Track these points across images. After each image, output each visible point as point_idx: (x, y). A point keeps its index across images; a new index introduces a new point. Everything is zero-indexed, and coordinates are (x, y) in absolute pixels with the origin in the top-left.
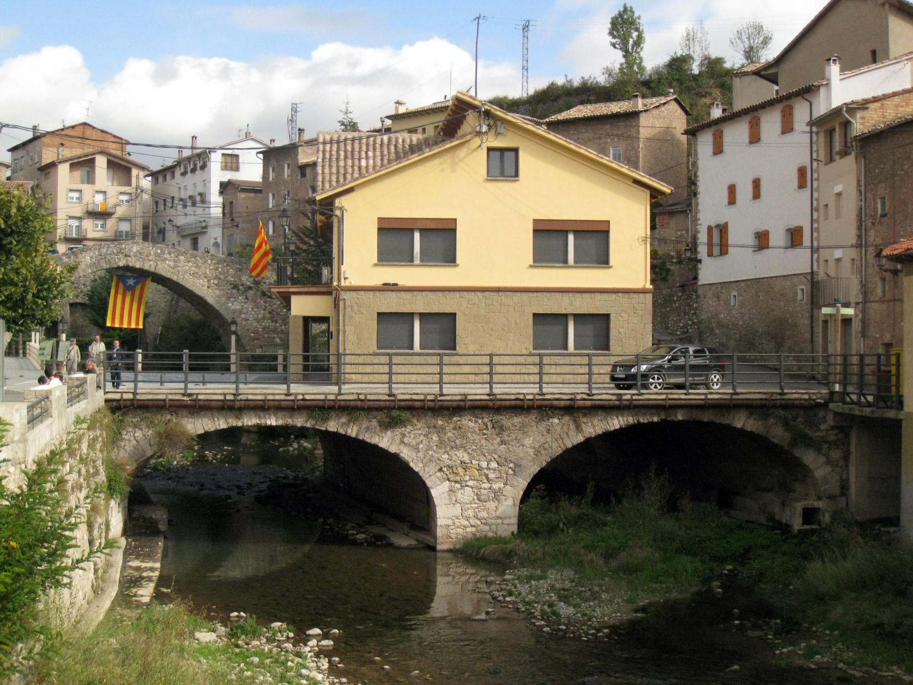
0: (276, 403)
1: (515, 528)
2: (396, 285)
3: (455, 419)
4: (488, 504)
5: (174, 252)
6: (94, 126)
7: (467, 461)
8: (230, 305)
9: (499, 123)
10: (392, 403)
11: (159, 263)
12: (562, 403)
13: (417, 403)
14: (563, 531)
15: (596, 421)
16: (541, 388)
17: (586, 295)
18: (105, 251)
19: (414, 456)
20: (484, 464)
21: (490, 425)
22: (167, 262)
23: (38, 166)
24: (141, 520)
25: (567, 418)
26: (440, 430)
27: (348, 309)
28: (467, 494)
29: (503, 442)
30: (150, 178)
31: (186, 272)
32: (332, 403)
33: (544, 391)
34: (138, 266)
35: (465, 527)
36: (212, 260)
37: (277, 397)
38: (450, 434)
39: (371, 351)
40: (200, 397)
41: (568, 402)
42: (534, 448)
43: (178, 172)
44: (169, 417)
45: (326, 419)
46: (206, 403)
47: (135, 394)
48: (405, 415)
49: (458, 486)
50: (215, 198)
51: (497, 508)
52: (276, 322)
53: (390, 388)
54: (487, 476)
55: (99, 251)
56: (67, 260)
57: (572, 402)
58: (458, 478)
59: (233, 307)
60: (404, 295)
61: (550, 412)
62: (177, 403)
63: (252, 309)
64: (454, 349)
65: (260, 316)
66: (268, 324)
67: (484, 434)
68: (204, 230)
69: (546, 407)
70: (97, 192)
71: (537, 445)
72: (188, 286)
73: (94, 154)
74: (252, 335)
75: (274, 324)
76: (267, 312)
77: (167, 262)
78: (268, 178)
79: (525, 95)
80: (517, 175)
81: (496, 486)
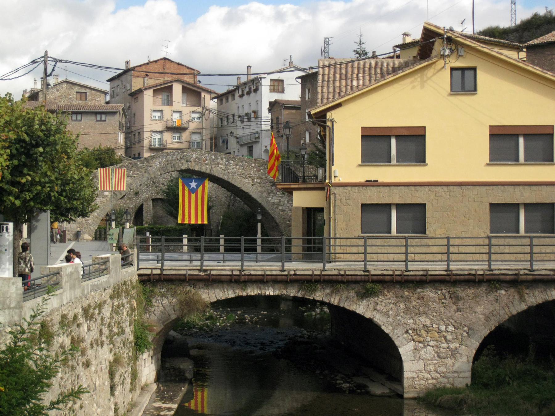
0: (273, 277)
1: (469, 381)
2: (376, 181)
3: (419, 290)
4: (446, 361)
6: (172, 60)
7: (429, 325)
8: (270, 199)
9: (459, 48)
10: (366, 277)
11: (213, 166)
12: (508, 278)
13: (386, 277)
14: (509, 384)
15: (537, 293)
16: (490, 265)
17: (534, 188)
18: (170, 157)
19: (385, 320)
20: (443, 328)
21: (447, 296)
22: (220, 166)
23: (129, 92)
24: (172, 370)
25: (512, 290)
26: (407, 300)
27: (338, 202)
28: (428, 352)
29: (458, 310)
30: (216, 100)
31: (235, 173)
32: (318, 277)
33: (493, 267)
34: (196, 169)
35: (427, 379)
37: (274, 273)
38: (415, 303)
39: (356, 235)
40: (213, 272)
41: (512, 277)
42: (485, 315)
43: (237, 95)
44: (189, 288)
45: (314, 290)
46: (218, 277)
47: (162, 270)
48: (378, 287)
49: (421, 345)
50: (265, 114)
51: (453, 364)
53: (365, 265)
54: (445, 337)
55: (166, 158)
56: (141, 165)
57: (516, 277)
58: (421, 339)
59: (272, 201)
60: (383, 189)
61: (497, 285)
62: (195, 277)
64: (425, 233)
67: (443, 303)
68: (257, 140)
69: (494, 280)
70: (174, 111)
71: (487, 312)
72: (236, 184)
73: (171, 82)
77: (220, 166)
78: (305, 98)
79: (513, 25)
80: (475, 89)
81: (452, 346)
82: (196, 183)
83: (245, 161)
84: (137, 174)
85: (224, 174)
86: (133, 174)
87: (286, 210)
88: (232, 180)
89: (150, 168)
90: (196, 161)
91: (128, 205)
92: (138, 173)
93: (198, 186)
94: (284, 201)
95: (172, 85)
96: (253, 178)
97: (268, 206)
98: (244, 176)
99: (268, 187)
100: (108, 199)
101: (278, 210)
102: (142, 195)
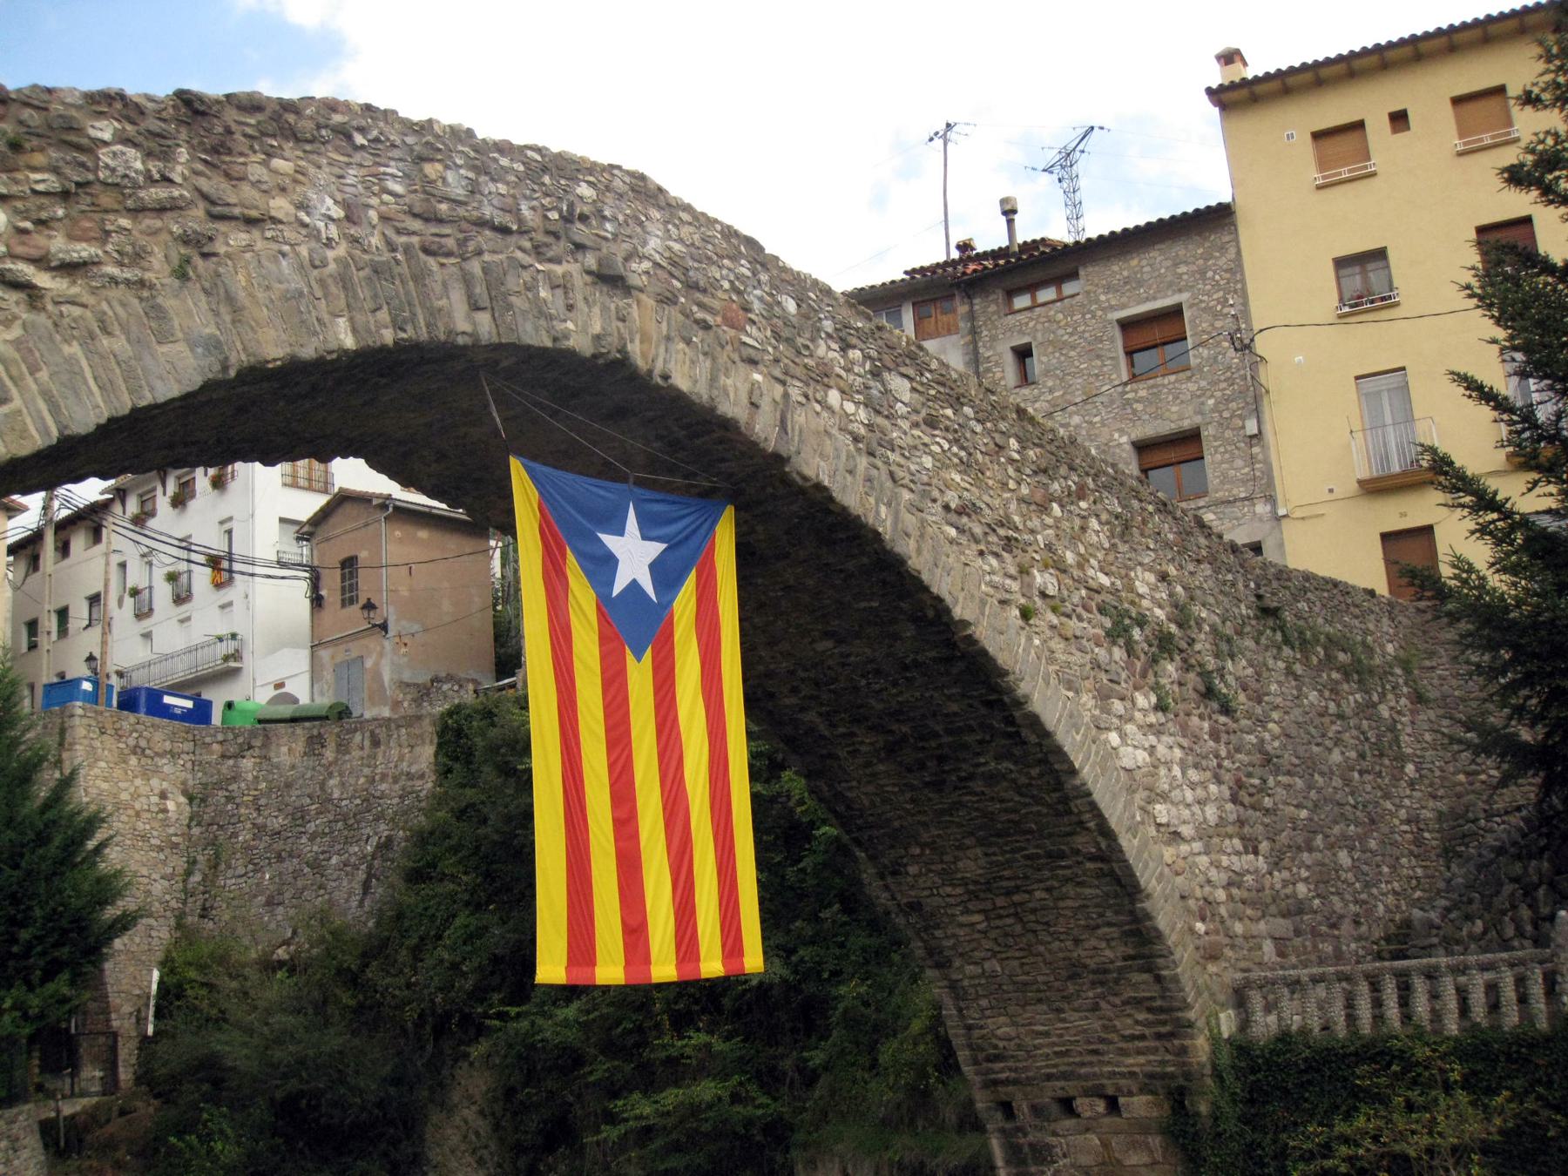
68: (233, 664)
77: (834, 397)
82: (656, 548)
84: (70, 268)
89: (238, 238)
93: (666, 574)
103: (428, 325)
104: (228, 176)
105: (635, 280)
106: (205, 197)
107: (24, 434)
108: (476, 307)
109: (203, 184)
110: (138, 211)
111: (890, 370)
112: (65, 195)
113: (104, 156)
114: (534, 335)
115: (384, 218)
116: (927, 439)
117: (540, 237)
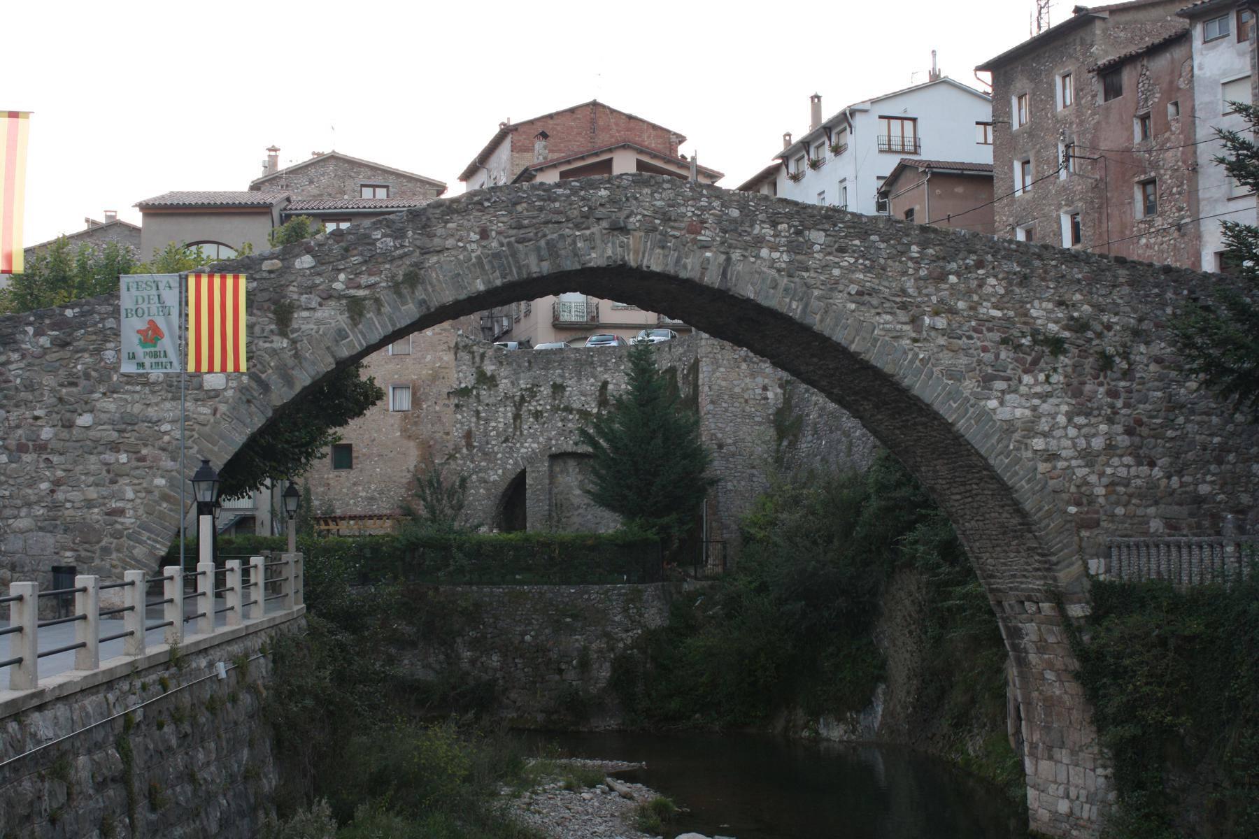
5: (789, 216)
11: (736, 255)
22: (764, 252)
31: (833, 286)
34: (656, 267)
36: (924, 245)
52: (1152, 464)
56: (390, 242)
59: (1004, 414)
63: (1070, 416)
65: (1098, 443)
66: (1122, 472)
72: (839, 336)
73: (610, 150)
74: (1072, 509)
75: (1145, 469)
76: (1119, 428)
78: (1009, 125)
83: (877, 232)
85: (786, 290)
86: (350, 284)
87: (1064, 453)
88: (821, 321)
90: (655, 229)
91: (480, 475)
92: (373, 280)
94: (1053, 416)
95: (611, 160)
96: (914, 311)
97: (987, 436)
98: (875, 302)
99: (985, 349)
100: (223, 408)
101: (1029, 454)
102: (522, 446)
103: (518, 273)
104: (428, 236)
105: (630, 226)
106: (419, 247)
107: (354, 347)
108: (541, 260)
109: (418, 243)
110: (391, 261)
111: (809, 229)
112: (365, 262)
113: (378, 244)
114: (570, 265)
115: (499, 233)
116: (837, 260)
117: (579, 220)
